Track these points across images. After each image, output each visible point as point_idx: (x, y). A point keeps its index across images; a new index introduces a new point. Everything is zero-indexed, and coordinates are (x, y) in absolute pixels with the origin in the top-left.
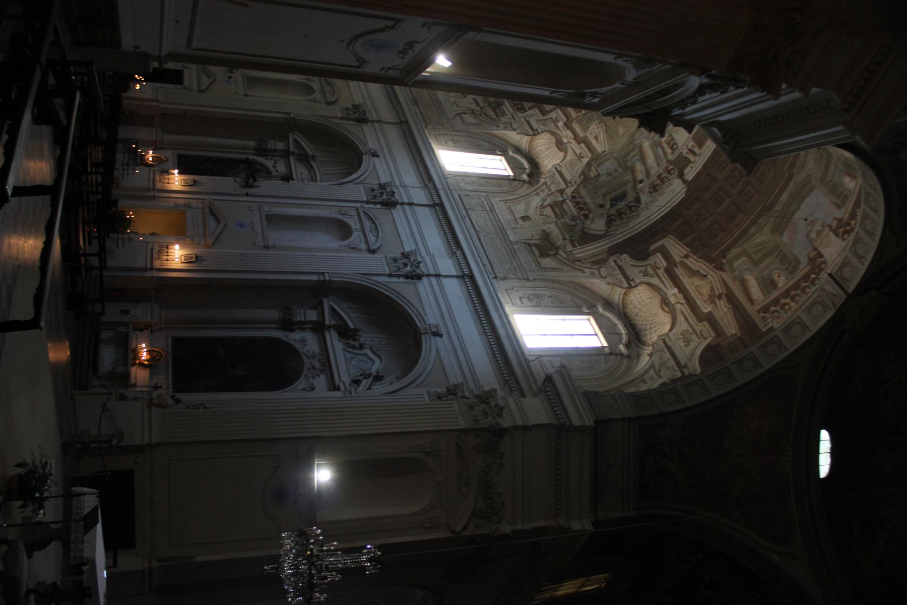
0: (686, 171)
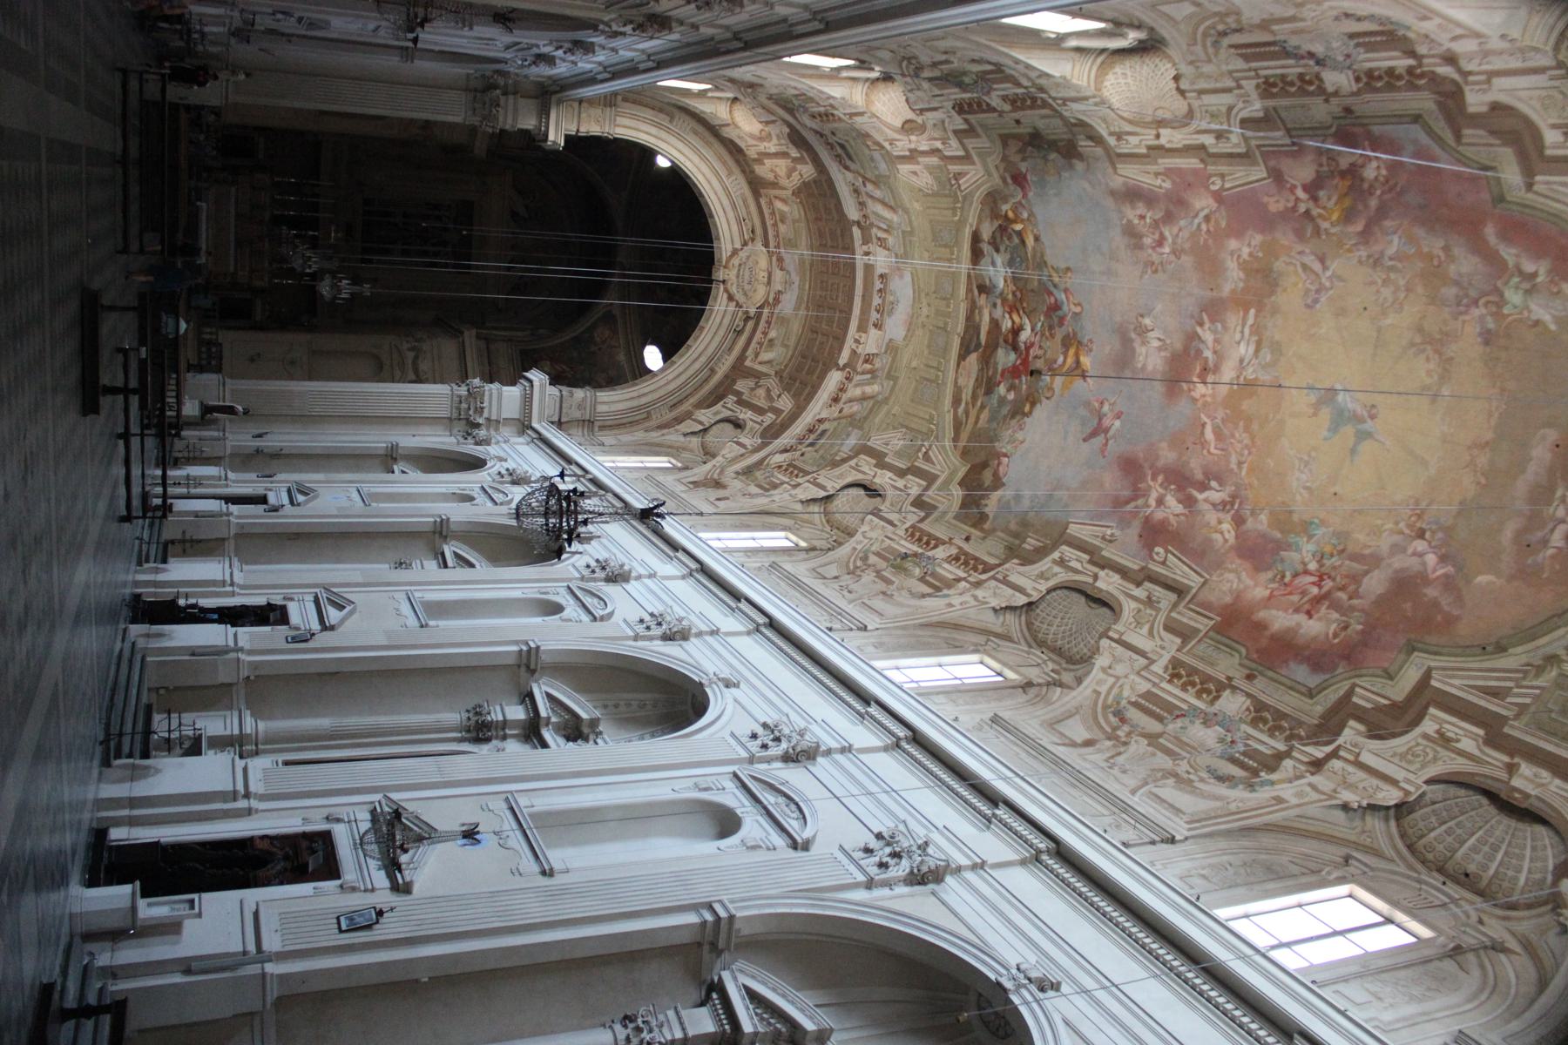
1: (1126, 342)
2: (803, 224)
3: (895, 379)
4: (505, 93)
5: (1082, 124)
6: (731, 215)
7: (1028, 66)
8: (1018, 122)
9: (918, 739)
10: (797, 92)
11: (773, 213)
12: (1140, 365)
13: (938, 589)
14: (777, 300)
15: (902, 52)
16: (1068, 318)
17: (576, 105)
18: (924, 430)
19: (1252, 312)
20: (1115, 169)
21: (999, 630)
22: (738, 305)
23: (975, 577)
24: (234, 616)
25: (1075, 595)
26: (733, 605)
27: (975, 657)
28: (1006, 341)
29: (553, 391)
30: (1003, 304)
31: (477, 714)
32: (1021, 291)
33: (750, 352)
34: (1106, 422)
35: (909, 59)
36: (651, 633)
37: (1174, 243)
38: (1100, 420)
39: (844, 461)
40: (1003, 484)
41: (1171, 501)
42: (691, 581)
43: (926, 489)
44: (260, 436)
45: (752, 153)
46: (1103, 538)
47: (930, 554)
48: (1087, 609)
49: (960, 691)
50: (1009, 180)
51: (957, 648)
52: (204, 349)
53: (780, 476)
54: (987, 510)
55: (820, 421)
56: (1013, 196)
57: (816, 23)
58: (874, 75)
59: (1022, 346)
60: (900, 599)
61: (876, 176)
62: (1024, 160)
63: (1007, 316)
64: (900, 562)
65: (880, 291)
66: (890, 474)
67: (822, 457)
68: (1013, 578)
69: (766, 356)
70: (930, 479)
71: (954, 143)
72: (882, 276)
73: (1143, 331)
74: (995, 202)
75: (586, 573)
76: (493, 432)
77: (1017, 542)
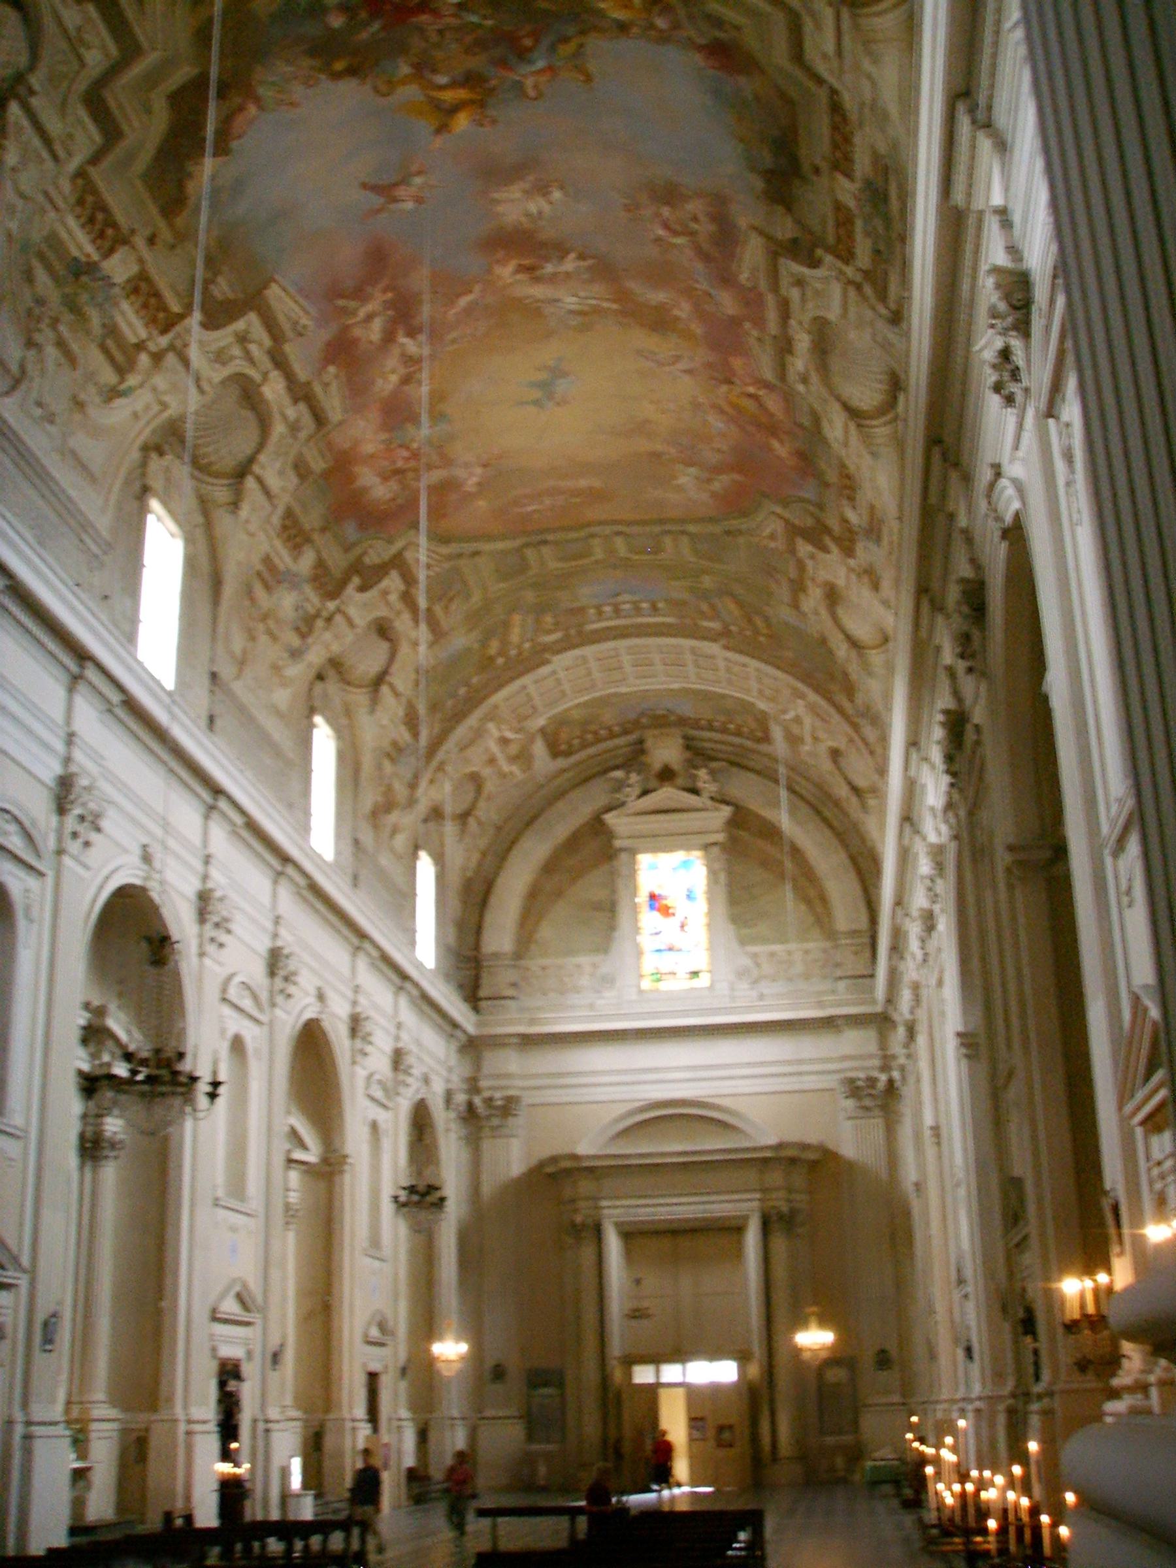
12: (496, 196)
19: (615, 306)
34: (401, 192)
41: (377, 325)
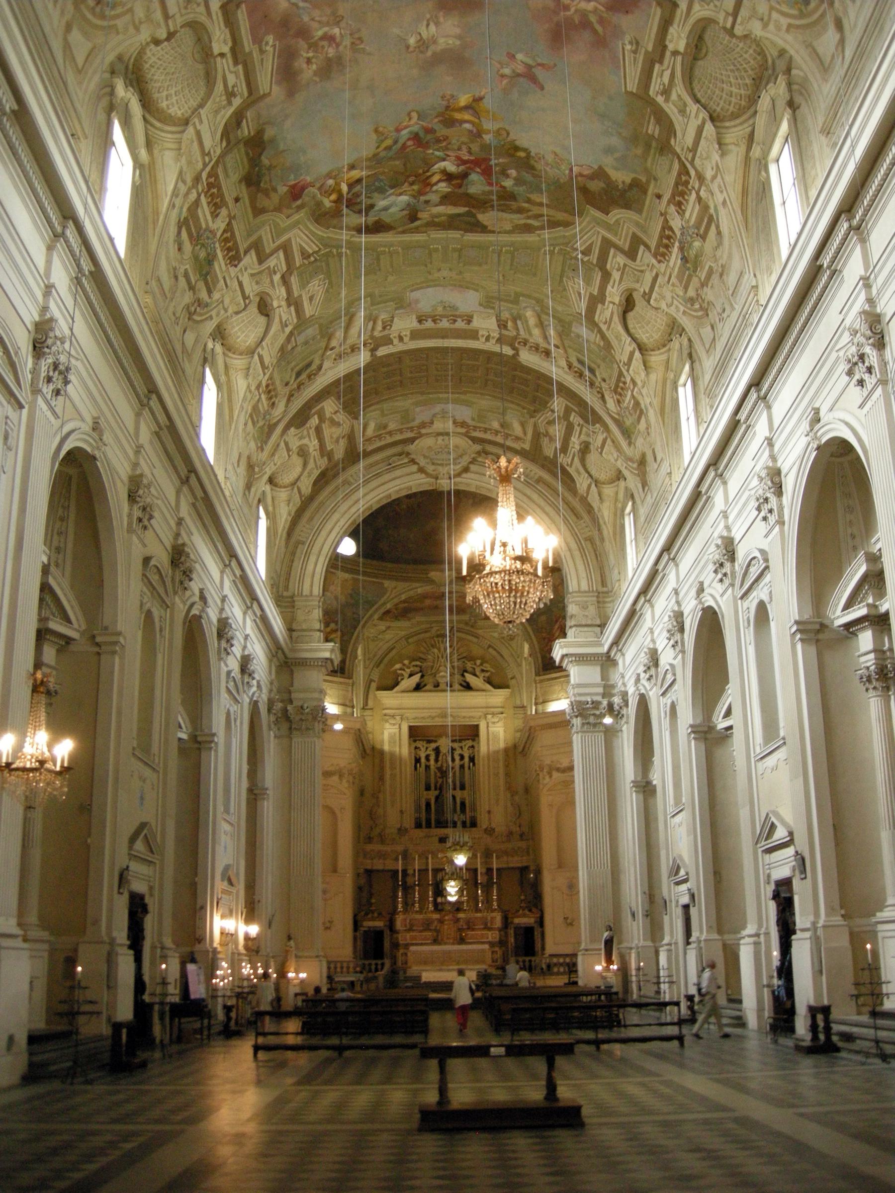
0: (380, 349)
1: (439, 59)
2: (385, 406)
3: (517, 295)
4: (291, 701)
5: (226, 134)
6: (387, 477)
7: (175, 194)
8: (237, 200)
9: (847, 207)
10: (250, 423)
11: (379, 437)
12: (458, 43)
13: (711, 219)
14: (463, 424)
15: (184, 320)
16: (424, 124)
17: (295, 634)
18: (561, 258)
20: (265, 96)
21: (743, 148)
22: (473, 461)
23: (694, 182)
24: (787, 930)
25: (697, 72)
26: (744, 426)
27: (772, 168)
28: (460, 186)
29: (570, 633)
30: (425, 194)
31: (869, 680)
32: (408, 177)
33: (516, 446)
34: (520, 69)
35: (190, 315)
36: (775, 508)
37: (328, 24)
38: (519, 75)
39: (603, 337)
40: (600, 168)
42: (727, 475)
43: (617, 248)
44: (633, 915)
45: (323, 463)
46: (635, 52)
47: (678, 233)
48: (710, 55)
49: (804, 176)
50: (299, 202)
51: (765, 188)
52: (555, 970)
53: (627, 401)
54: (628, 181)
55: (570, 366)
56: (314, 197)
57: (152, 403)
58: (219, 349)
59: (462, 168)
60: (725, 257)
61: (322, 337)
62: (275, 190)
63: (435, 188)
64: (690, 263)
65: (434, 321)
66: (609, 287)
67: (604, 360)
68: (689, 141)
69: (517, 429)
70: (607, 245)
71: (272, 262)
72: (420, 321)
73: (423, 45)
74: (325, 214)
75: (727, 582)
76: (616, 691)
77: (654, 144)
